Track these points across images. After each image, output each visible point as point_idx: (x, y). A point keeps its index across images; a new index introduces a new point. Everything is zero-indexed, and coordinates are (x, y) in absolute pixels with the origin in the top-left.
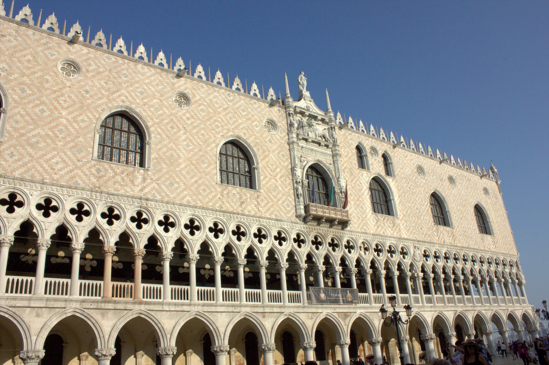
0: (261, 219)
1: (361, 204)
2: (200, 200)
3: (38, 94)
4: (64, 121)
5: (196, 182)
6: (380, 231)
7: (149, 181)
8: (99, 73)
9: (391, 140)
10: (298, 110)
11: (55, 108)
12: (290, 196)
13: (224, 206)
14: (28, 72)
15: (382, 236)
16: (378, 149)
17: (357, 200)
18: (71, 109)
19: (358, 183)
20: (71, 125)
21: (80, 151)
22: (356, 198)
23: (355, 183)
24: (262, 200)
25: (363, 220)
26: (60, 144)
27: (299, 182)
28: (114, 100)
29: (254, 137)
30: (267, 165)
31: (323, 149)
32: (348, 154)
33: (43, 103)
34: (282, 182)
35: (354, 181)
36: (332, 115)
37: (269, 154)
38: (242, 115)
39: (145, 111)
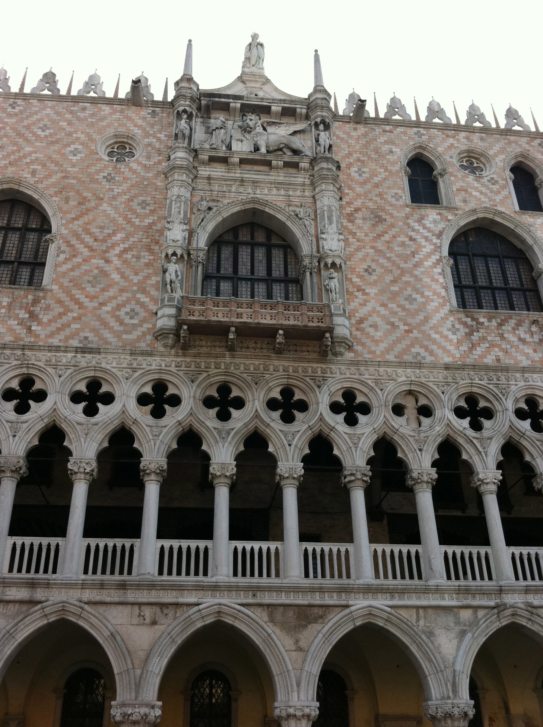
0: (27, 352)
6: (482, 357)
12: (144, 291)
15: (487, 368)
16: (491, 152)
17: (394, 281)
22: (388, 278)
23: (388, 242)
24: (48, 308)
25: (407, 331)
27: (174, 254)
29: (59, 175)
31: (280, 176)
32: (374, 174)
34: (125, 261)
35: (387, 237)
37: (101, 205)
38: (38, 137)
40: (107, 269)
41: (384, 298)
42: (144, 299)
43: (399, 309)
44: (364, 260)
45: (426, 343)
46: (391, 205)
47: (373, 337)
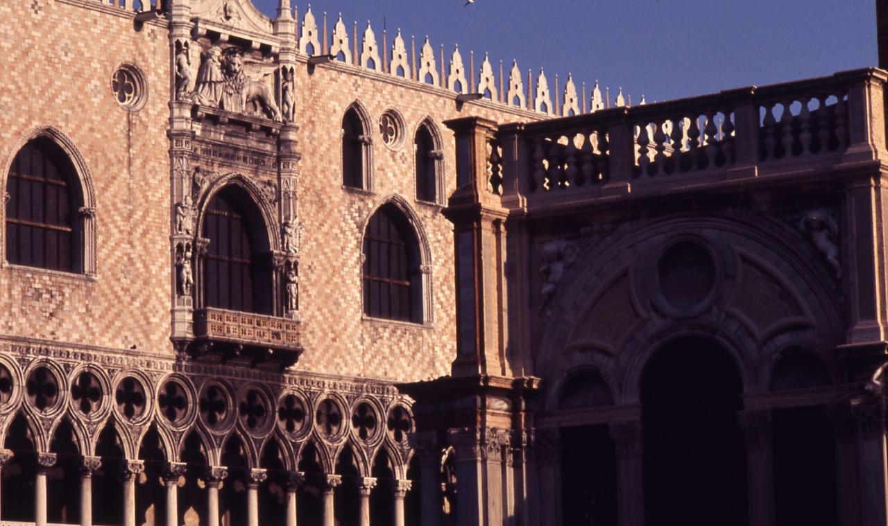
1: (336, 295)
9: (452, 79)
10: (202, 29)
12: (161, 286)
13: (14, 324)
16: (406, 115)
17: (328, 282)
19: (336, 230)
22: (324, 278)
23: (327, 234)
25: (334, 340)
29: (88, 125)
34: (145, 247)
35: (325, 229)
36: (291, 29)
37: (120, 171)
40: (132, 256)
41: (319, 301)
43: (328, 315)
44: (308, 255)
45: (343, 353)
46: (331, 186)
47: (311, 344)
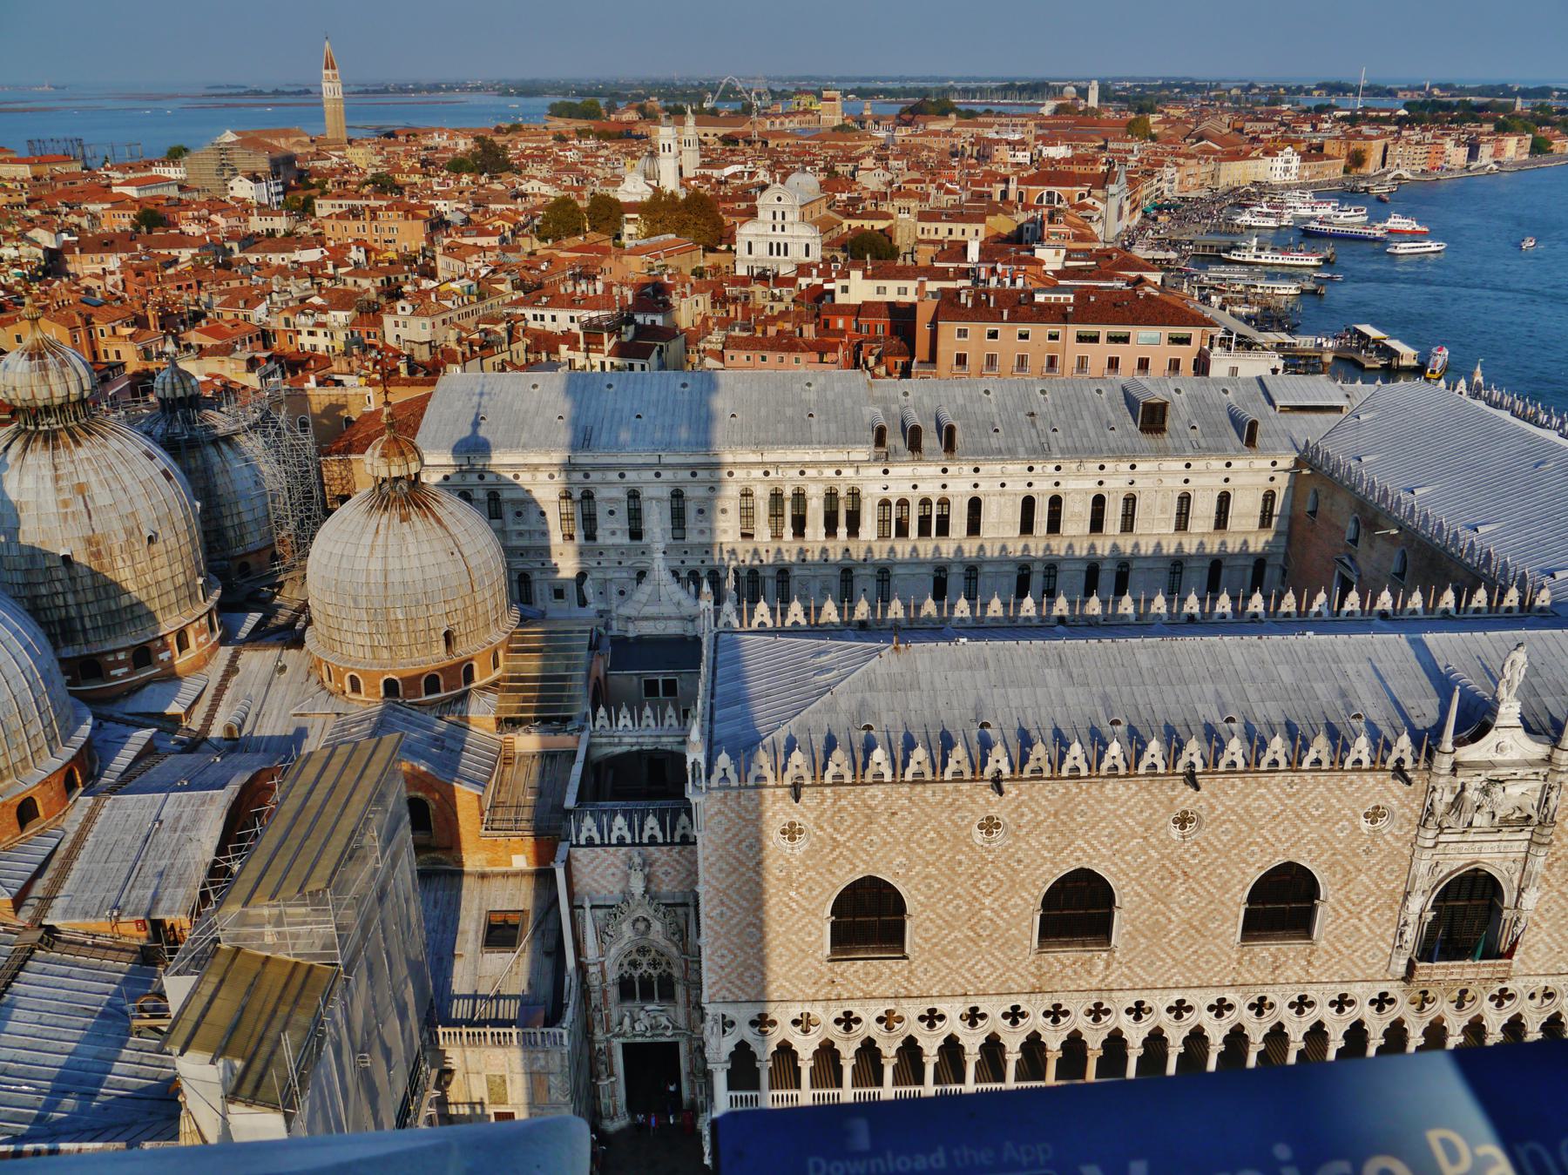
2: (1199, 978)
3: (950, 885)
4: (988, 913)
5: (1195, 952)
7: (1115, 965)
8: (1038, 824)
11: (975, 898)
12: (1383, 940)
14: (930, 859)
18: (996, 894)
20: (1001, 917)
21: (1012, 948)
24: (1319, 957)
26: (984, 944)
28: (1063, 861)
30: (1348, 898)
33: (958, 896)
34: (1373, 919)
39: (1115, 864)
42: (1381, 944)
